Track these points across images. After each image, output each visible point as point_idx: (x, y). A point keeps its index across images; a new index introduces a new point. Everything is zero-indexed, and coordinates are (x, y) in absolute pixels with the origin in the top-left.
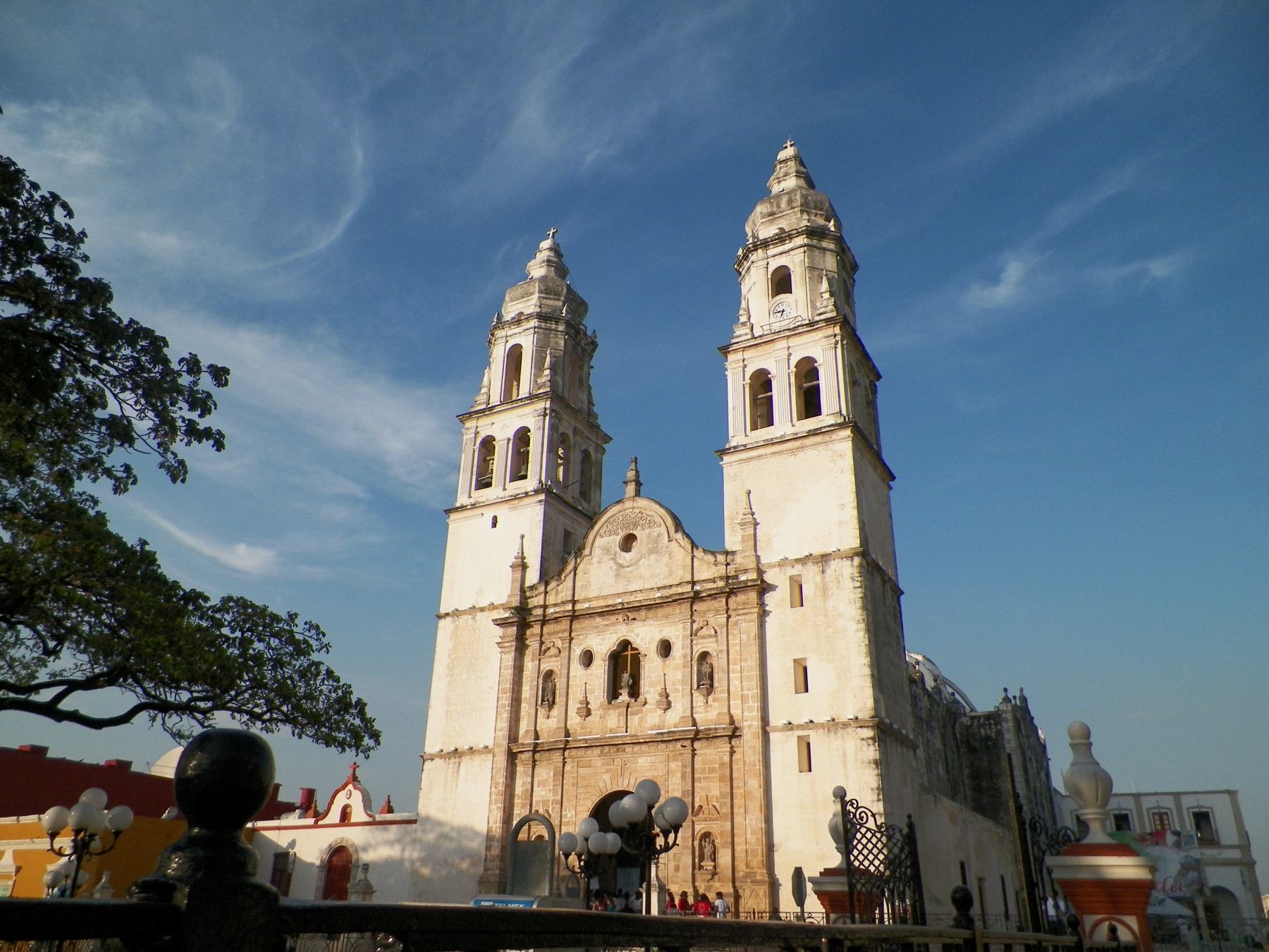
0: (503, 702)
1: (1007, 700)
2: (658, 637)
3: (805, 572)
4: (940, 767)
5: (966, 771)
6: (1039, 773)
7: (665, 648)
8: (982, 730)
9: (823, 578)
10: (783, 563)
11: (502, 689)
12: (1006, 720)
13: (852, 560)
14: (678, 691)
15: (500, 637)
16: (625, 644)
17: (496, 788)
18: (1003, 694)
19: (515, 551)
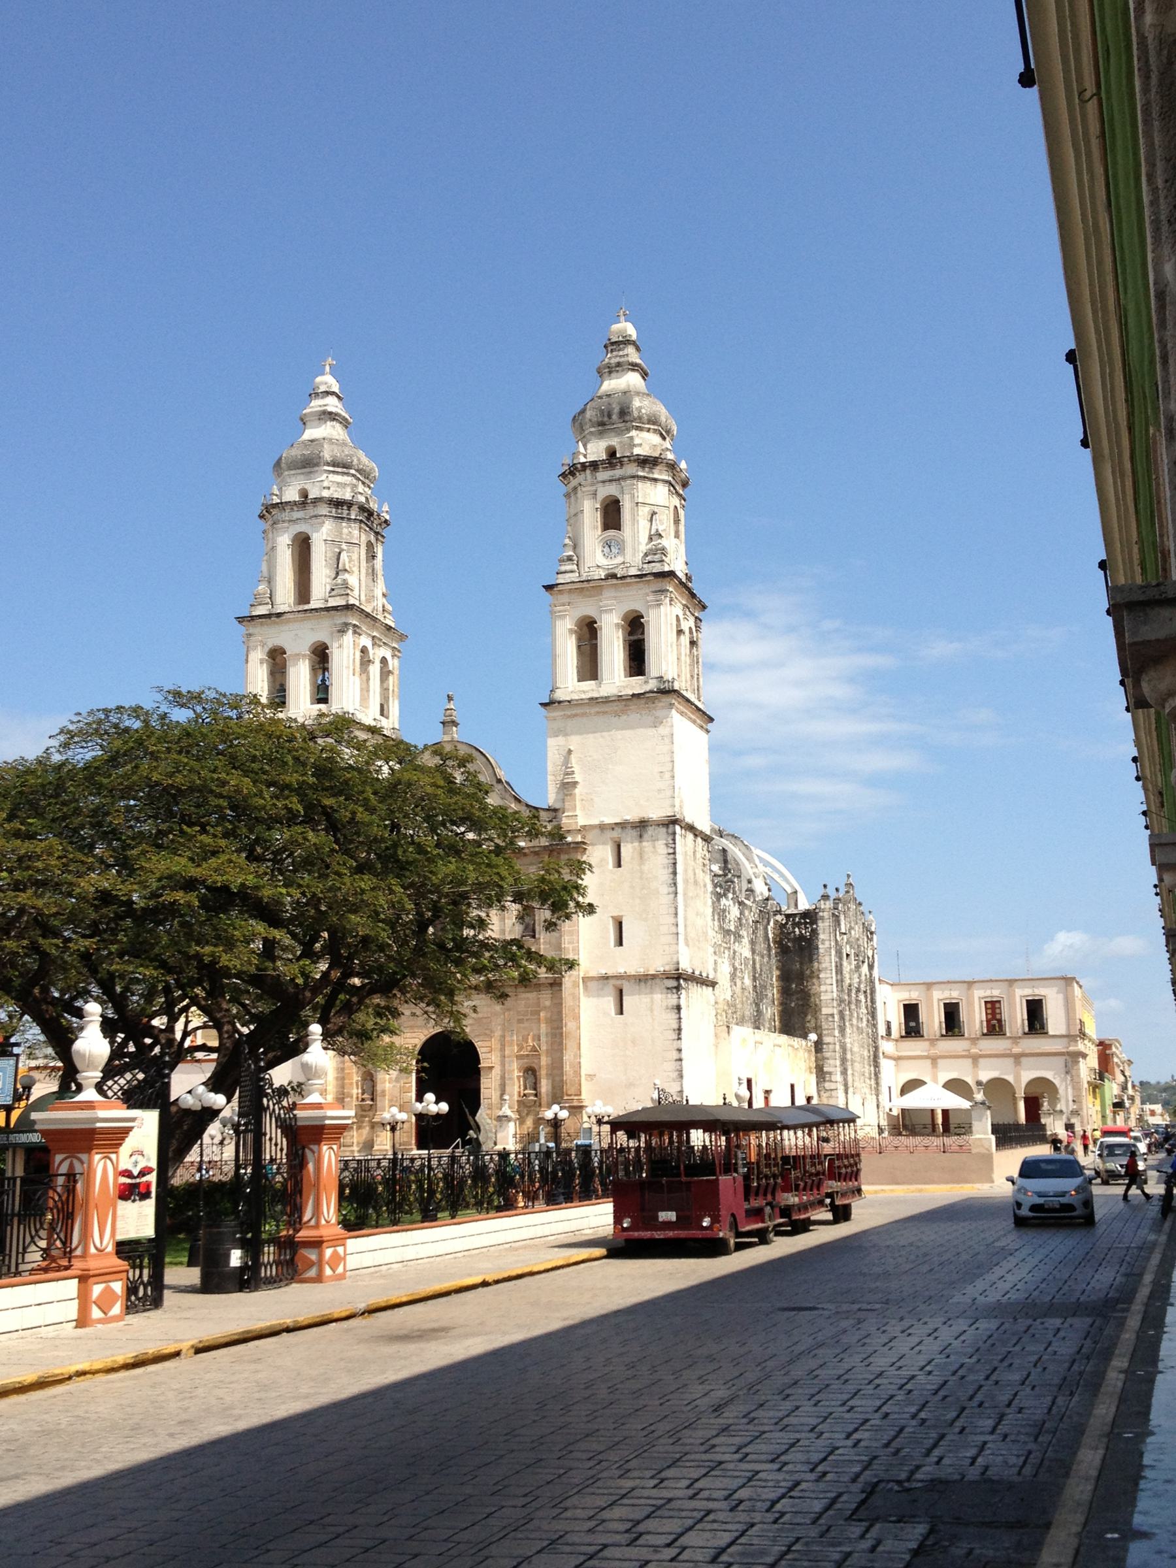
1: (825, 897)
3: (624, 835)
4: (746, 976)
5: (776, 973)
6: (858, 967)
8: (797, 930)
12: (822, 918)
13: (668, 828)
18: (822, 891)
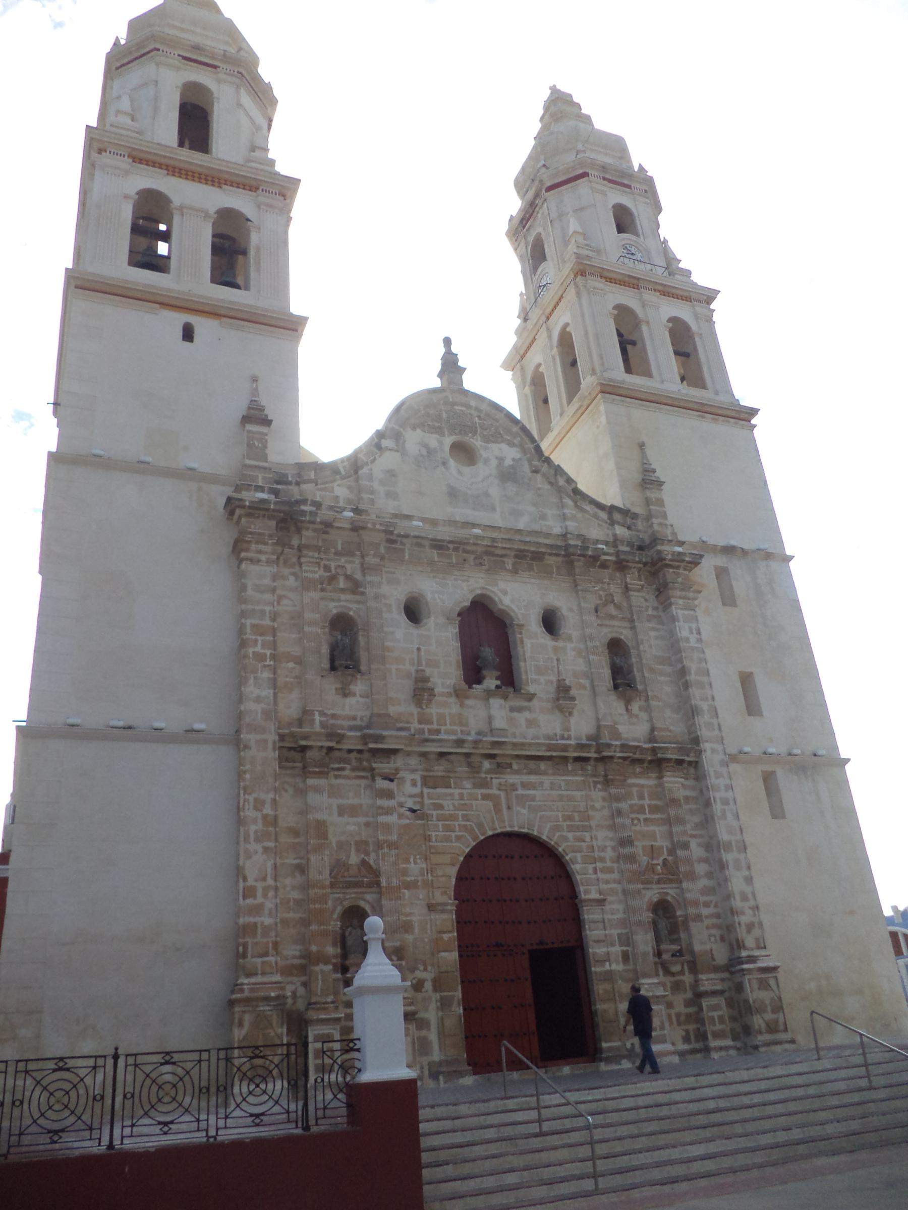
0: (258, 649)
7: (550, 622)
11: (254, 626)
14: (584, 687)
17: (256, 809)
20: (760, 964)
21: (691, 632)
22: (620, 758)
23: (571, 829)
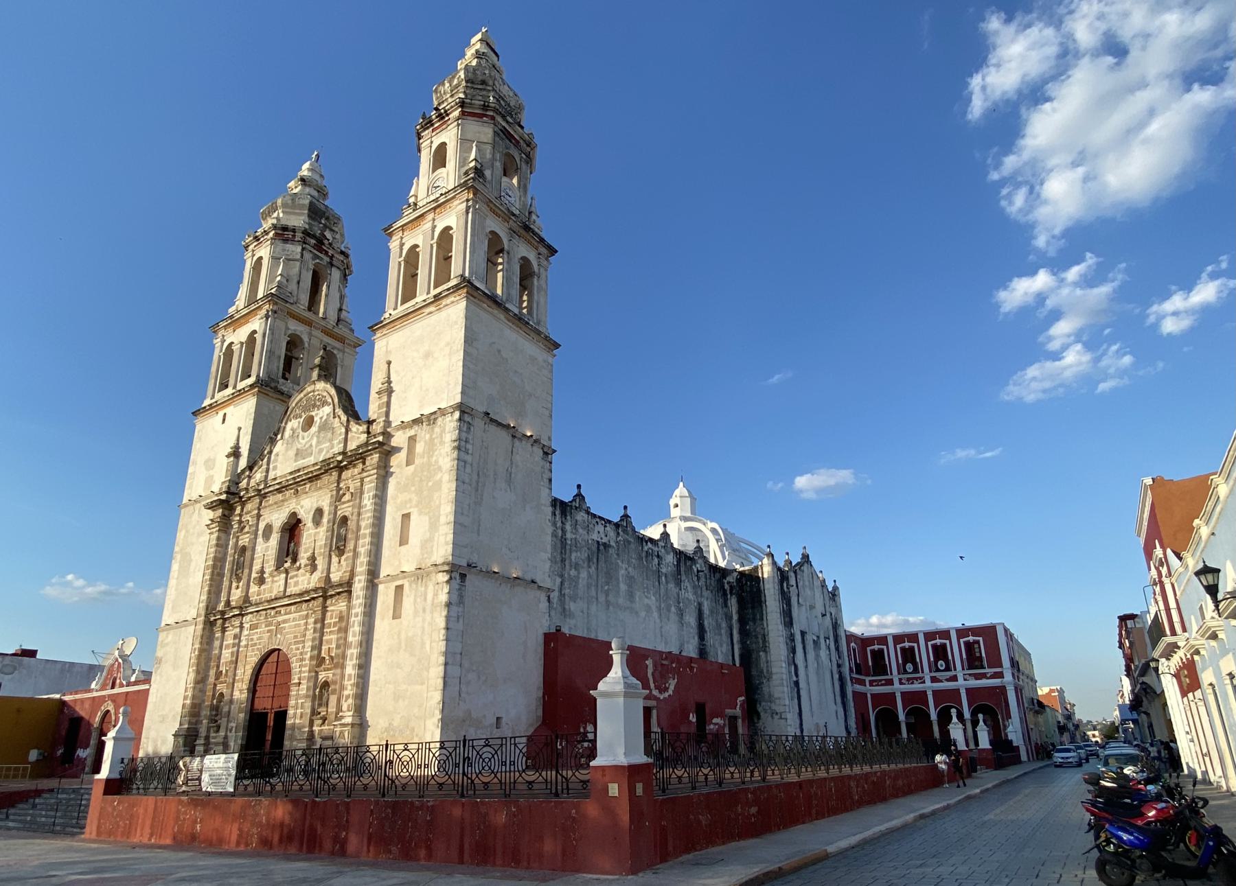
2: (315, 506)
9: (431, 436)
10: (403, 426)
15: (212, 520)
16: (294, 514)
19: (232, 443)
20: (343, 721)
21: (369, 499)
22: (320, 596)
23: (296, 643)
